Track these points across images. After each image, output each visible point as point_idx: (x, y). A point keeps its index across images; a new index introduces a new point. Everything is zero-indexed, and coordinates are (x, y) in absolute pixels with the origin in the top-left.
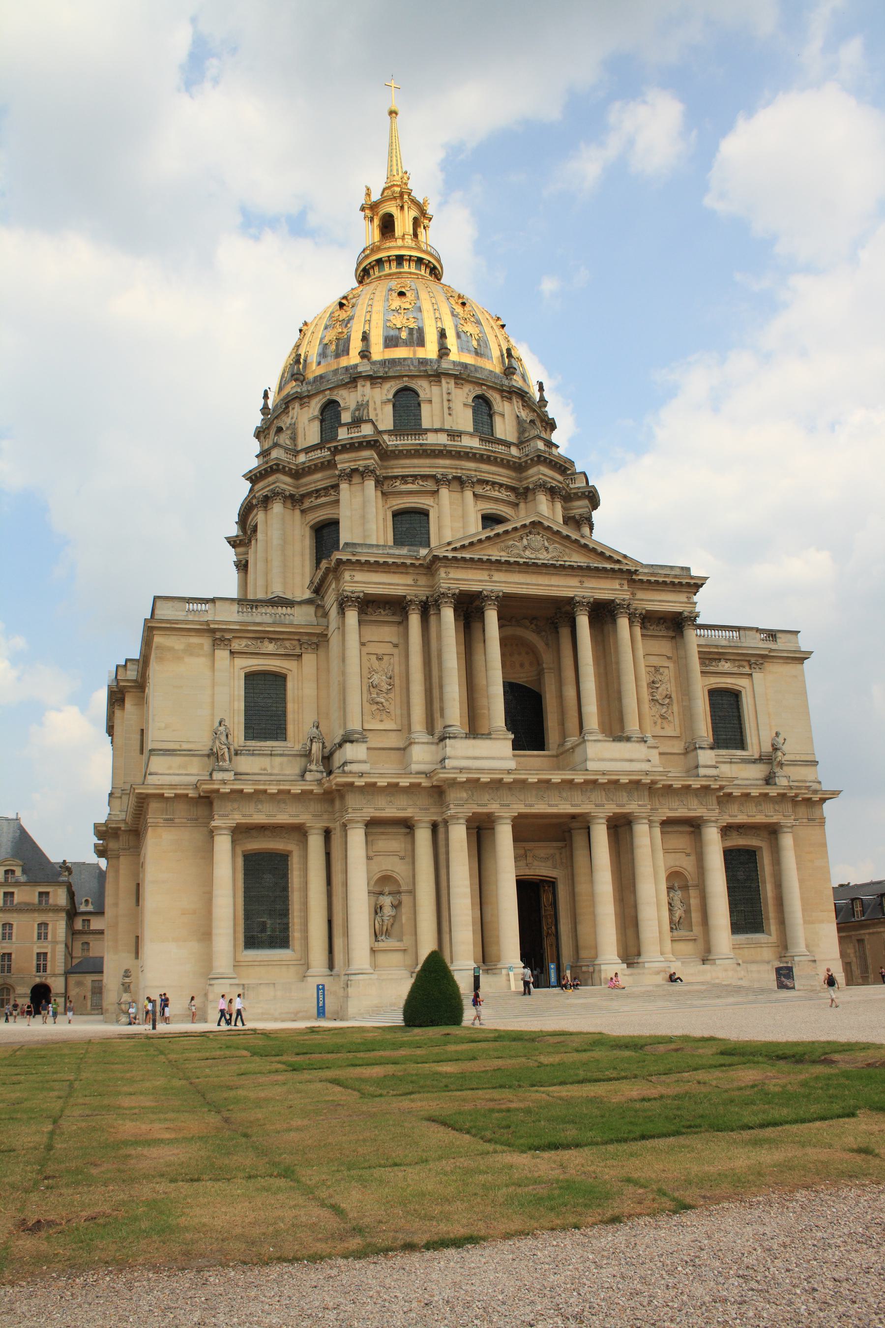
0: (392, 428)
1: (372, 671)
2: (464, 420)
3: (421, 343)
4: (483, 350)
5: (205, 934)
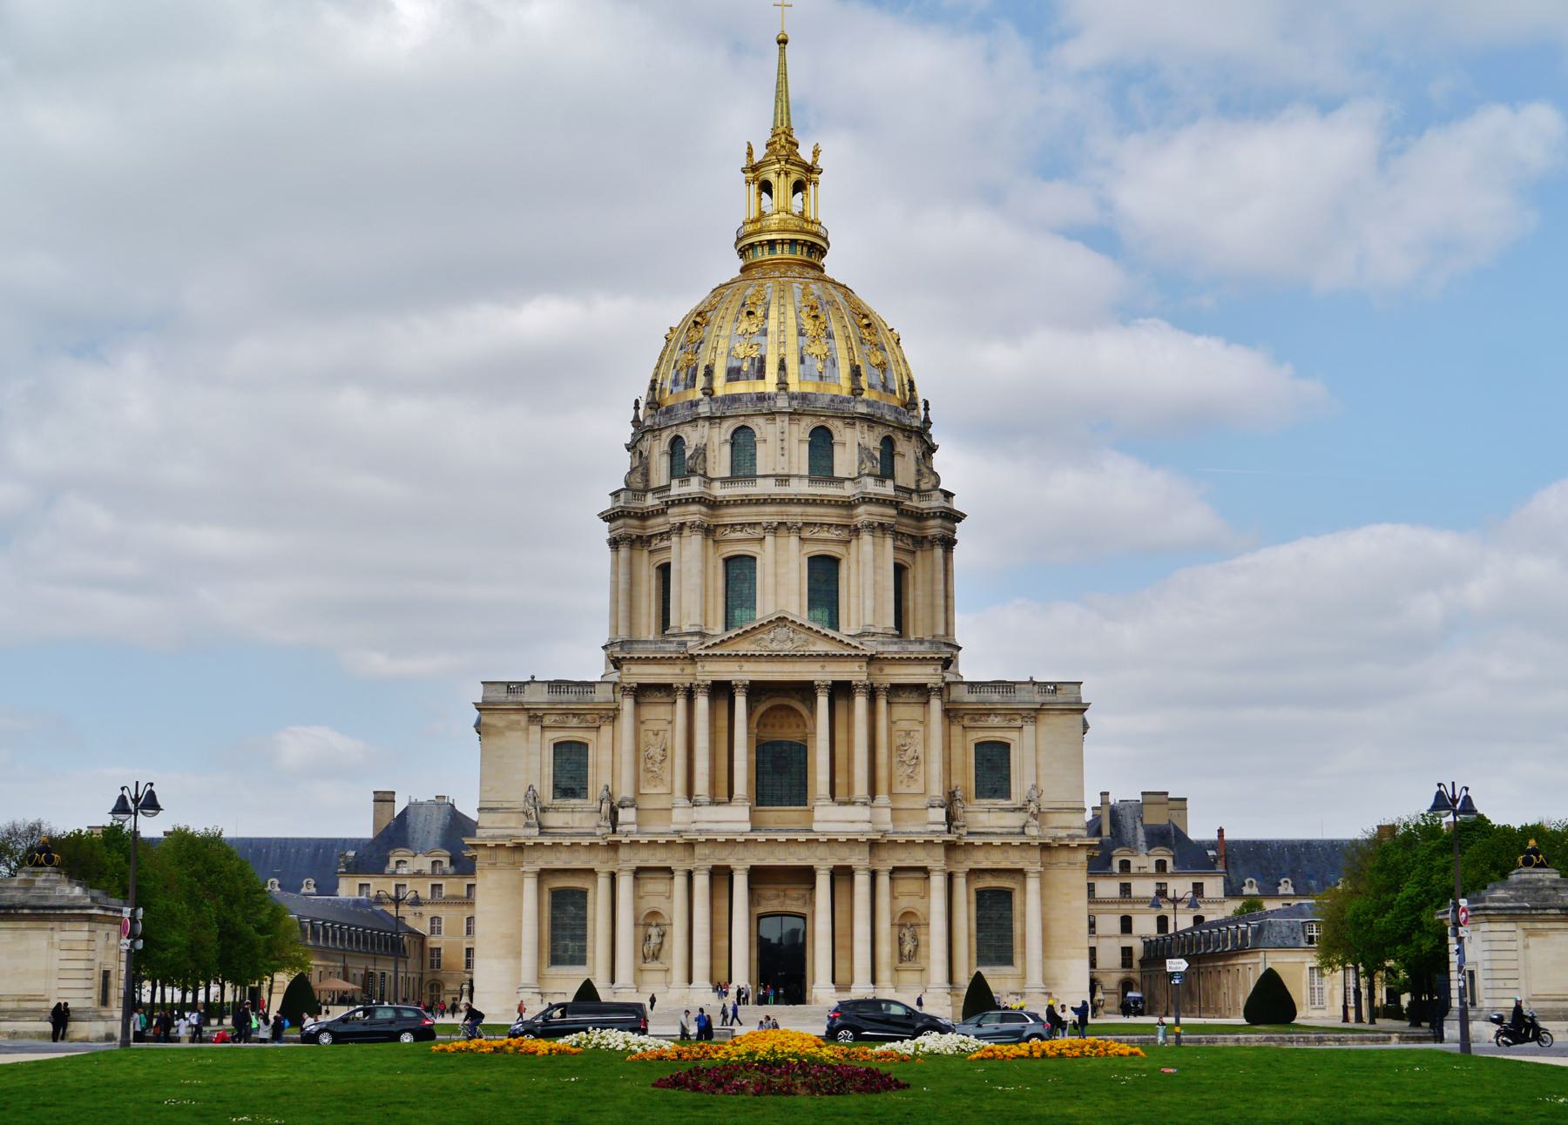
0: (728, 474)
1: (648, 745)
2: (800, 459)
3: (761, 375)
4: (826, 373)
5: (518, 955)
